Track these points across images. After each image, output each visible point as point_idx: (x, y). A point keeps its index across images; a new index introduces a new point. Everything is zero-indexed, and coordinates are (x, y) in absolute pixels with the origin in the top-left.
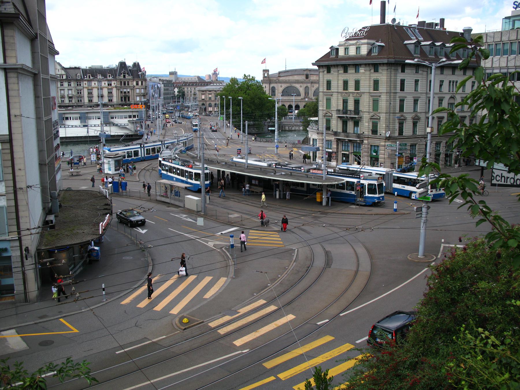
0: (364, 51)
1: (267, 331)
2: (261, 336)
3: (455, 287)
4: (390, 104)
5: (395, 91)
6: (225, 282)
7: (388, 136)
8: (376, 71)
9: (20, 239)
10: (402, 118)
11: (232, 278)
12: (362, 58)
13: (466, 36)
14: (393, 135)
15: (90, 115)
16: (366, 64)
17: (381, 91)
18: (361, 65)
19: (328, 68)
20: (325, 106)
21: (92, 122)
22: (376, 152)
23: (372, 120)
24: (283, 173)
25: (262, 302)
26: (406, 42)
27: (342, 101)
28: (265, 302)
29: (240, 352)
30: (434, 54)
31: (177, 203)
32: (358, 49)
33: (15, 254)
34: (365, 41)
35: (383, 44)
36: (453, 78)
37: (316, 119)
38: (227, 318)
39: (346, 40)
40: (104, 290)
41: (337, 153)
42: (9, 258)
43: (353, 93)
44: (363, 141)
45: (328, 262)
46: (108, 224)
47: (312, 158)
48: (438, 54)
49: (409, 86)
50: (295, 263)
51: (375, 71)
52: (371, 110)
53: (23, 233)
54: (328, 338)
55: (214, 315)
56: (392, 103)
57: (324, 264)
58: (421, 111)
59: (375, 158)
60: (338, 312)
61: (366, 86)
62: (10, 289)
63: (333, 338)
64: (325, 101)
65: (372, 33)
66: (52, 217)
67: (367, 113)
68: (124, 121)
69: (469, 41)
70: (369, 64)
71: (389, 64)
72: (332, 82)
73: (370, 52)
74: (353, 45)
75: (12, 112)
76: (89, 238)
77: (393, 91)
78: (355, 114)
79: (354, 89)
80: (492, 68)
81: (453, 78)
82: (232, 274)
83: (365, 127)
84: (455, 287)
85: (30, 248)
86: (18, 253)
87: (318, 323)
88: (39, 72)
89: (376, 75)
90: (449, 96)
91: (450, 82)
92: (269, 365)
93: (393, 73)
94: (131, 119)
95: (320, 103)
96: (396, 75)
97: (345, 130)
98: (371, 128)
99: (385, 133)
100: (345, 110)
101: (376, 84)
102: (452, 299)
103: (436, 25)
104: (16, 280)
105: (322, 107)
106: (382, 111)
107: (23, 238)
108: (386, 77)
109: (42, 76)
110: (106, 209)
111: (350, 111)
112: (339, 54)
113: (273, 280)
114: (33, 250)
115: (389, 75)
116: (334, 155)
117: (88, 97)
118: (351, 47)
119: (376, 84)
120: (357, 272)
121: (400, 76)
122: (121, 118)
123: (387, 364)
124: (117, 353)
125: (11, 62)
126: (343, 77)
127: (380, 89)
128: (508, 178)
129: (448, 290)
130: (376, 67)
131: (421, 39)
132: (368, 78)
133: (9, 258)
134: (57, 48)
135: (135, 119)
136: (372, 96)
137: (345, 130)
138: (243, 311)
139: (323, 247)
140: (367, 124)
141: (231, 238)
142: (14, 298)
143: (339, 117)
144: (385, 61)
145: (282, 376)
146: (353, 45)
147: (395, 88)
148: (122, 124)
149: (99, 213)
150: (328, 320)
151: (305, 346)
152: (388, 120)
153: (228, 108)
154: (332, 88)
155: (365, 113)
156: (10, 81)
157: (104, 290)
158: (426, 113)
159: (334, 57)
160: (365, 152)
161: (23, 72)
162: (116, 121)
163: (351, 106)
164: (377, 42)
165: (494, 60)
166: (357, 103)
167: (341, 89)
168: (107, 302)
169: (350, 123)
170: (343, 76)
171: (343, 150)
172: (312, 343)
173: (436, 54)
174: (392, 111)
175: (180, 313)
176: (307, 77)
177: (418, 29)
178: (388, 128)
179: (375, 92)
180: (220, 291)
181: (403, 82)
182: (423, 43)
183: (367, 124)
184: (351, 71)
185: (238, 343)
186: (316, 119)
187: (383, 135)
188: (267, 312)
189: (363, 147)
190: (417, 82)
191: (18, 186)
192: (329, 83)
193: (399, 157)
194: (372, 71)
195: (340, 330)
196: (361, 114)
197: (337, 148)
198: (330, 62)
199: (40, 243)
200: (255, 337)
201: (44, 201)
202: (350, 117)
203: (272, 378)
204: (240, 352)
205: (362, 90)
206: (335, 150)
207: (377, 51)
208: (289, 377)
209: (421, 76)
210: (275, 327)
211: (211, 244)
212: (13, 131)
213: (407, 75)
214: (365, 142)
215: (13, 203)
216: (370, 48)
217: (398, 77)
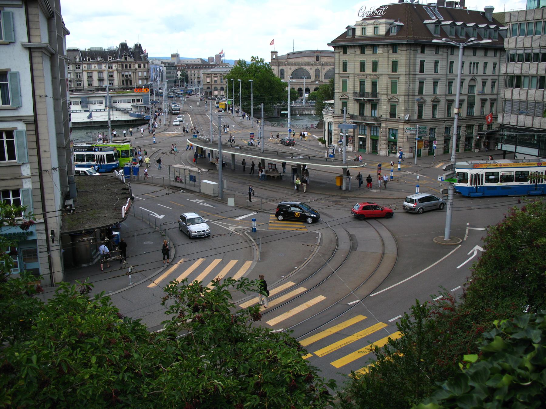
0: (382, 31)
1: (299, 311)
2: (294, 316)
3: (515, 243)
4: (409, 86)
5: (414, 73)
7: (407, 119)
8: (395, 51)
9: (45, 222)
10: (422, 100)
11: (258, 261)
12: (380, 38)
13: (488, 15)
14: (412, 118)
15: (91, 100)
16: (384, 45)
17: (399, 73)
18: (378, 45)
19: (345, 49)
20: (341, 89)
21: (93, 107)
22: (394, 136)
23: (390, 103)
24: (301, 157)
25: (290, 284)
26: (425, 22)
27: (359, 83)
28: (293, 284)
30: (454, 34)
31: (192, 188)
32: (376, 28)
33: (41, 237)
34: (384, 20)
35: (402, 24)
36: (474, 59)
37: (332, 102)
39: (364, 19)
41: (353, 137)
42: (35, 241)
43: (370, 75)
44: (381, 124)
45: (353, 247)
46: (129, 208)
47: (327, 143)
48: (459, 35)
49: (429, 67)
50: (320, 247)
51: (393, 52)
52: (390, 93)
53: (48, 215)
54: (361, 318)
56: (411, 85)
57: (349, 247)
58: (441, 94)
59: (393, 142)
60: (368, 293)
61: (384, 67)
62: (36, 273)
63: (366, 317)
64: (341, 83)
65: (389, 12)
66: (70, 202)
67: (385, 96)
68: (128, 106)
69: (491, 21)
70: (387, 45)
71: (408, 45)
72: (348, 64)
73: (388, 32)
74: (371, 24)
75: (37, 93)
76: (112, 222)
77: (412, 73)
78: (373, 96)
79: (371, 70)
80: (516, 48)
81: (474, 59)
82: (257, 257)
83: (383, 110)
84: (516, 244)
85: (55, 231)
86: (44, 237)
87: (350, 304)
88: (56, 52)
89: (395, 56)
90: (470, 78)
91: (471, 63)
93: (412, 53)
94: (135, 104)
95: (336, 86)
96: (415, 57)
97: (362, 113)
98: (389, 111)
99: (404, 116)
100: (362, 92)
101: (395, 65)
102: (512, 256)
103: (457, 3)
104: (42, 265)
105: (338, 89)
106: (401, 93)
107: (49, 220)
108: (405, 58)
109: (59, 56)
110: (125, 193)
111: (368, 93)
113: (300, 263)
114: (57, 232)
115: (408, 56)
116: (350, 139)
117: (88, 81)
118: (368, 26)
119: (395, 65)
120: (383, 255)
121: (420, 57)
122: (124, 102)
123: (509, 269)
125: (36, 40)
126: (360, 58)
127: (398, 70)
129: (509, 247)
130: (394, 47)
131: (441, 18)
132: (386, 59)
133: (35, 241)
134: (67, 26)
135: (138, 103)
136: (390, 78)
137: (362, 113)
139: (346, 230)
140: (385, 107)
141: (253, 222)
142: (40, 282)
143: (356, 100)
144: (405, 41)
145: (319, 353)
146: (371, 24)
147: (415, 69)
148: (125, 108)
149: (118, 197)
152: (407, 103)
153: (236, 91)
154: (348, 70)
155: (384, 96)
156: (35, 60)
158: (445, 95)
159: (351, 37)
160: (383, 136)
161: (46, 53)
162: (120, 106)
163: (368, 88)
164: (396, 21)
165: (518, 40)
166: (374, 85)
167: (358, 71)
168: (133, 285)
169: (368, 106)
170: (360, 56)
171: (359, 134)
172: (345, 322)
173: (456, 35)
174: (411, 94)
176: (318, 58)
177: (438, 8)
178: (407, 111)
179: (395, 74)
181: (422, 63)
182: (443, 23)
183: (385, 107)
184: (369, 51)
186: (332, 102)
187: (402, 118)
188: (297, 293)
189: (380, 130)
190: (436, 63)
191: (43, 168)
192: (345, 65)
193: (418, 141)
194: (391, 51)
195: (373, 309)
196: (379, 97)
197: (354, 132)
198: (346, 43)
199: (62, 227)
200: (287, 317)
201: (62, 186)
202: (367, 99)
205: (380, 71)
206: (352, 134)
207: (395, 31)
209: (441, 57)
210: (307, 307)
211: (232, 229)
212: (38, 112)
213: (426, 57)
214: (383, 125)
215: (38, 186)
216: (388, 28)
217: (417, 59)
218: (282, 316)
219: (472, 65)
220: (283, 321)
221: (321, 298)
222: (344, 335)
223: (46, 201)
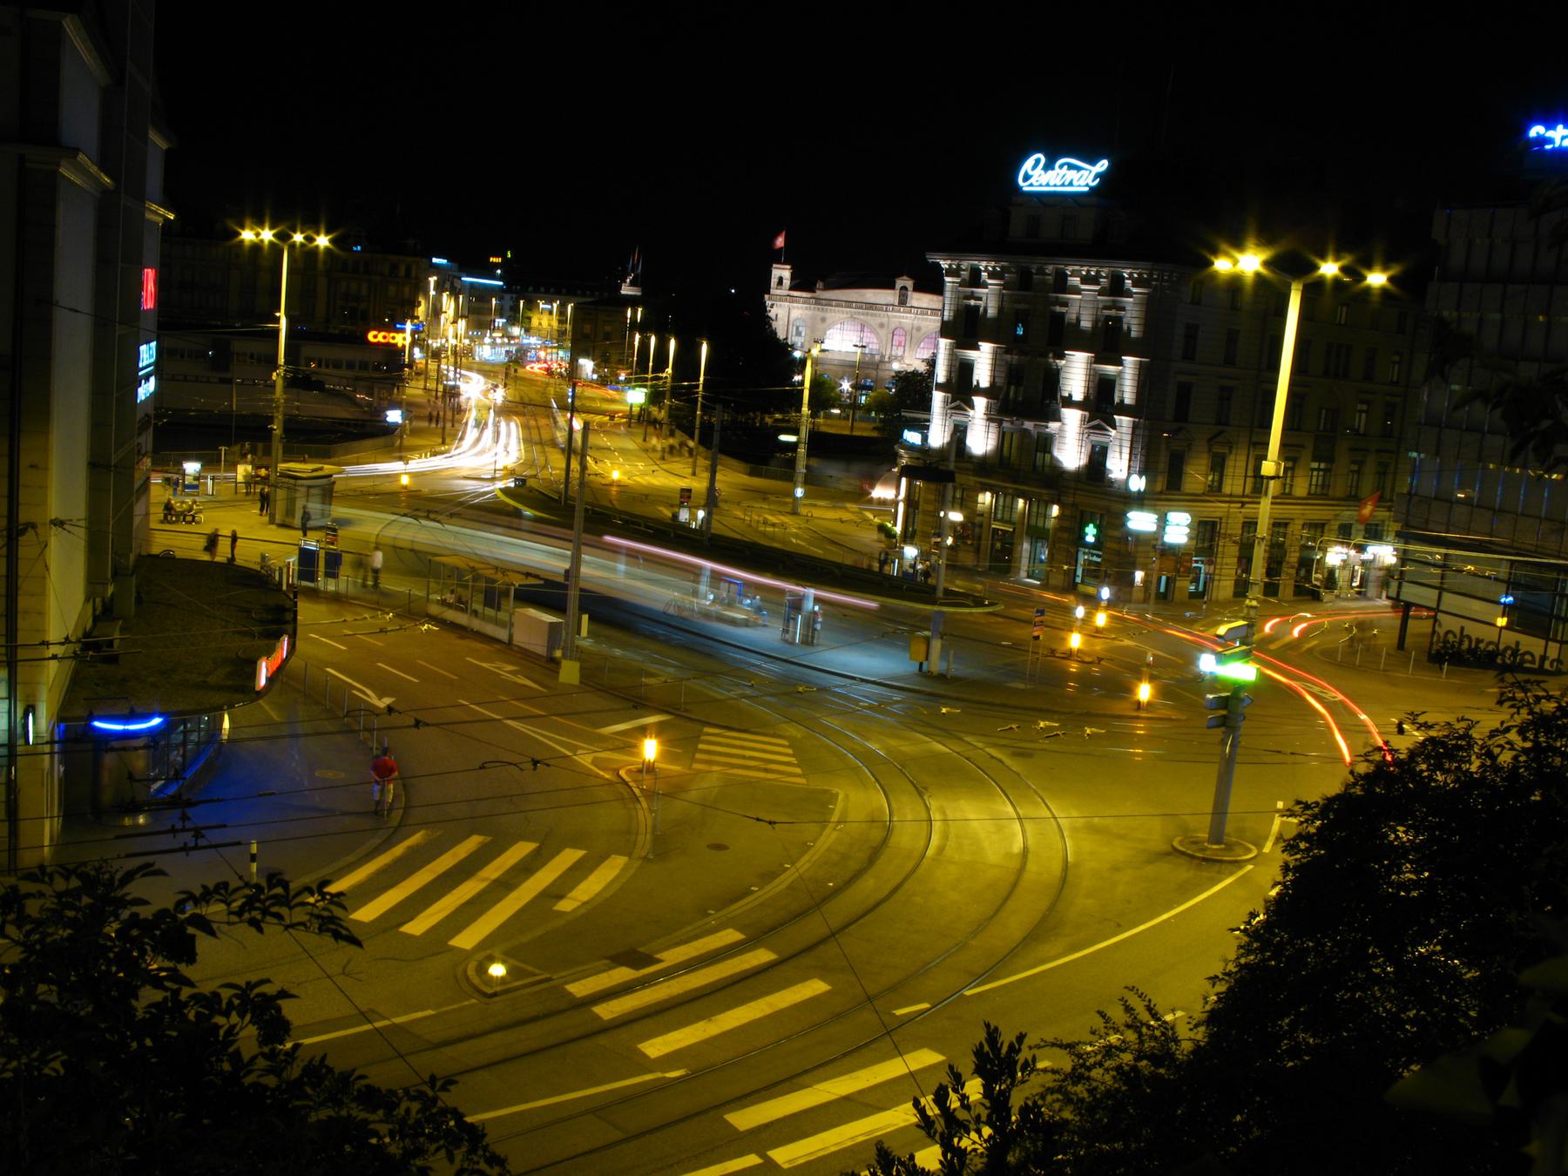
1: (744, 1021)
2: (725, 1034)
6: (624, 869)
11: (645, 858)
25: (731, 936)
29: (659, 1075)
31: (490, 629)
38: (623, 974)
40: (253, 858)
92: (745, 1119)
128: (1479, 641)
138: (672, 957)
145: (782, 1156)
150: (925, 1006)
151: (854, 1075)
157: (253, 858)
172: (876, 1068)
175: (481, 946)
180: (607, 895)
185: (655, 1048)
188: (746, 966)
200: (705, 1036)
201: (94, 580)
203: (752, 1160)
204: (659, 1075)
208: (801, 1161)
210: (768, 1011)
218: (701, 1025)
221: (816, 987)
222: (866, 1105)
223: (20, 616)
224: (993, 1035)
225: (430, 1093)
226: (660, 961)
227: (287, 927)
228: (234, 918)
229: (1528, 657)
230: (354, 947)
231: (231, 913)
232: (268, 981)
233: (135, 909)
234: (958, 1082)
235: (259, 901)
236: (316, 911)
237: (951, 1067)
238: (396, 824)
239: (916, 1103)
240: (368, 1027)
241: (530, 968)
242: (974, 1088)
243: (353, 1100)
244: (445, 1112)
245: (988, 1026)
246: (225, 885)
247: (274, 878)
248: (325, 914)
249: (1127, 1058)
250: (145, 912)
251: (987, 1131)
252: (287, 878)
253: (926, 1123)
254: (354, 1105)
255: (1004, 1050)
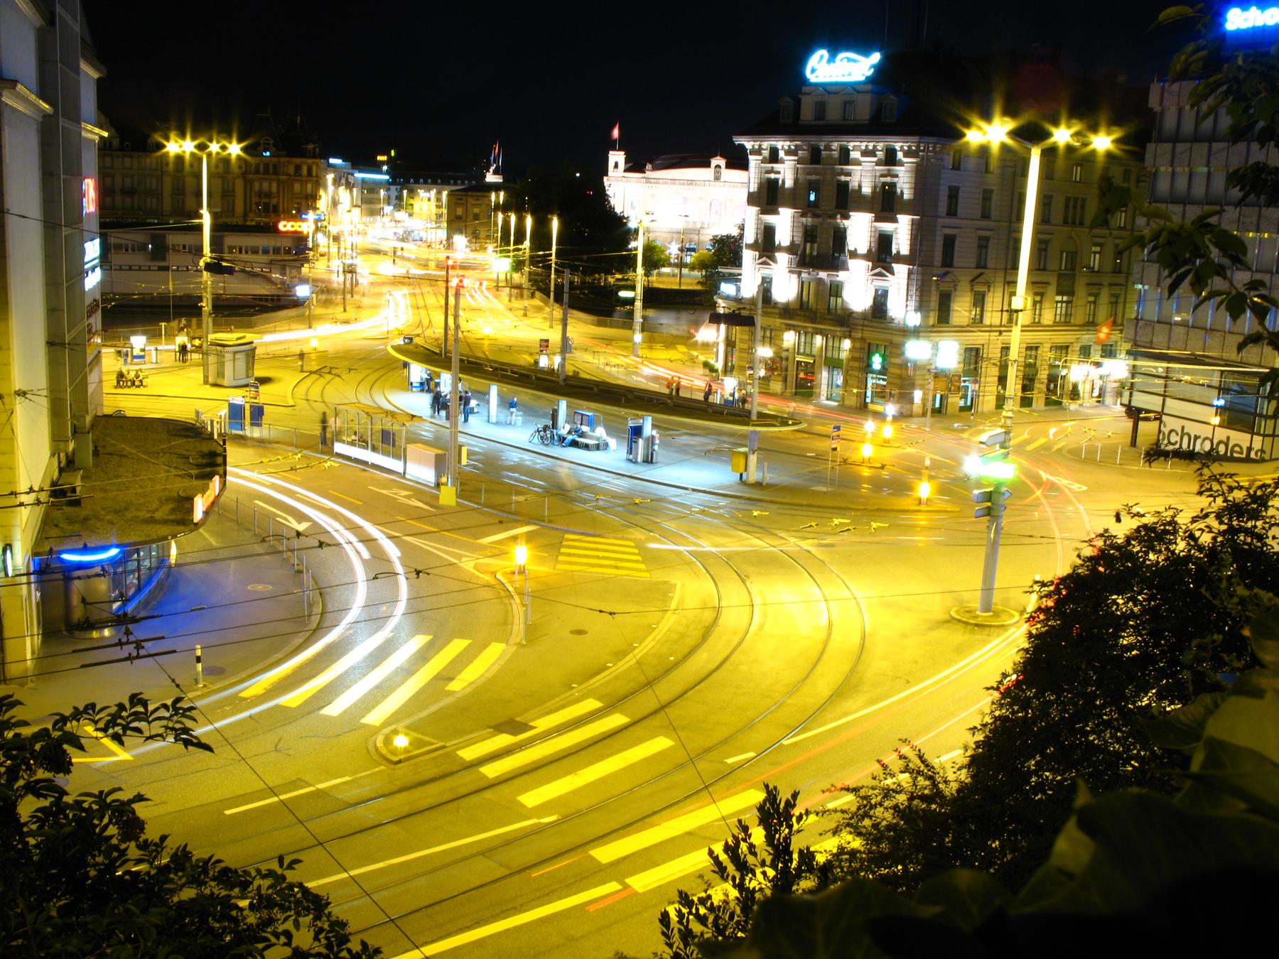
2: (588, 785)
25: (592, 704)
38: (504, 740)
40: (198, 660)
55: (472, 732)
87: (730, 761)
91: (1068, 199)
92: (605, 854)
112: (802, 117)
124: (228, 812)
128: (1196, 438)
138: (543, 724)
150: (752, 754)
157: (198, 660)
168: (206, 690)
175: (387, 723)
180: (489, 675)
185: (531, 799)
201: (57, 438)
203: (613, 886)
204: (535, 821)
210: (623, 765)
217: (942, 182)
218: (569, 778)
219: (1071, 204)
220: (560, 798)
221: (662, 743)
224: (772, 795)
225: (279, 871)
226: (533, 728)
227: (148, 738)
228: (100, 734)
229: (1237, 449)
230: (208, 753)
231: (96, 730)
232: (120, 789)
233: (18, 730)
234: (745, 829)
235: (121, 718)
236: (171, 725)
237: (740, 821)
238: (314, 626)
239: (711, 852)
240: (275, 799)
241: (427, 739)
242: (758, 835)
243: (213, 879)
244: (291, 887)
245: (767, 786)
246: (93, 706)
247: (136, 699)
248: (178, 726)
249: (902, 798)
250: (26, 732)
251: (771, 873)
252: (144, 696)
253: (720, 869)
254: (213, 884)
255: (782, 805)
